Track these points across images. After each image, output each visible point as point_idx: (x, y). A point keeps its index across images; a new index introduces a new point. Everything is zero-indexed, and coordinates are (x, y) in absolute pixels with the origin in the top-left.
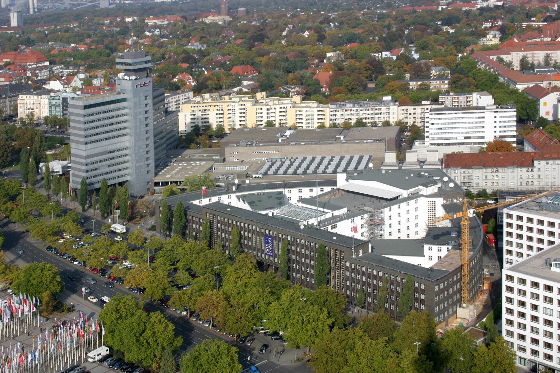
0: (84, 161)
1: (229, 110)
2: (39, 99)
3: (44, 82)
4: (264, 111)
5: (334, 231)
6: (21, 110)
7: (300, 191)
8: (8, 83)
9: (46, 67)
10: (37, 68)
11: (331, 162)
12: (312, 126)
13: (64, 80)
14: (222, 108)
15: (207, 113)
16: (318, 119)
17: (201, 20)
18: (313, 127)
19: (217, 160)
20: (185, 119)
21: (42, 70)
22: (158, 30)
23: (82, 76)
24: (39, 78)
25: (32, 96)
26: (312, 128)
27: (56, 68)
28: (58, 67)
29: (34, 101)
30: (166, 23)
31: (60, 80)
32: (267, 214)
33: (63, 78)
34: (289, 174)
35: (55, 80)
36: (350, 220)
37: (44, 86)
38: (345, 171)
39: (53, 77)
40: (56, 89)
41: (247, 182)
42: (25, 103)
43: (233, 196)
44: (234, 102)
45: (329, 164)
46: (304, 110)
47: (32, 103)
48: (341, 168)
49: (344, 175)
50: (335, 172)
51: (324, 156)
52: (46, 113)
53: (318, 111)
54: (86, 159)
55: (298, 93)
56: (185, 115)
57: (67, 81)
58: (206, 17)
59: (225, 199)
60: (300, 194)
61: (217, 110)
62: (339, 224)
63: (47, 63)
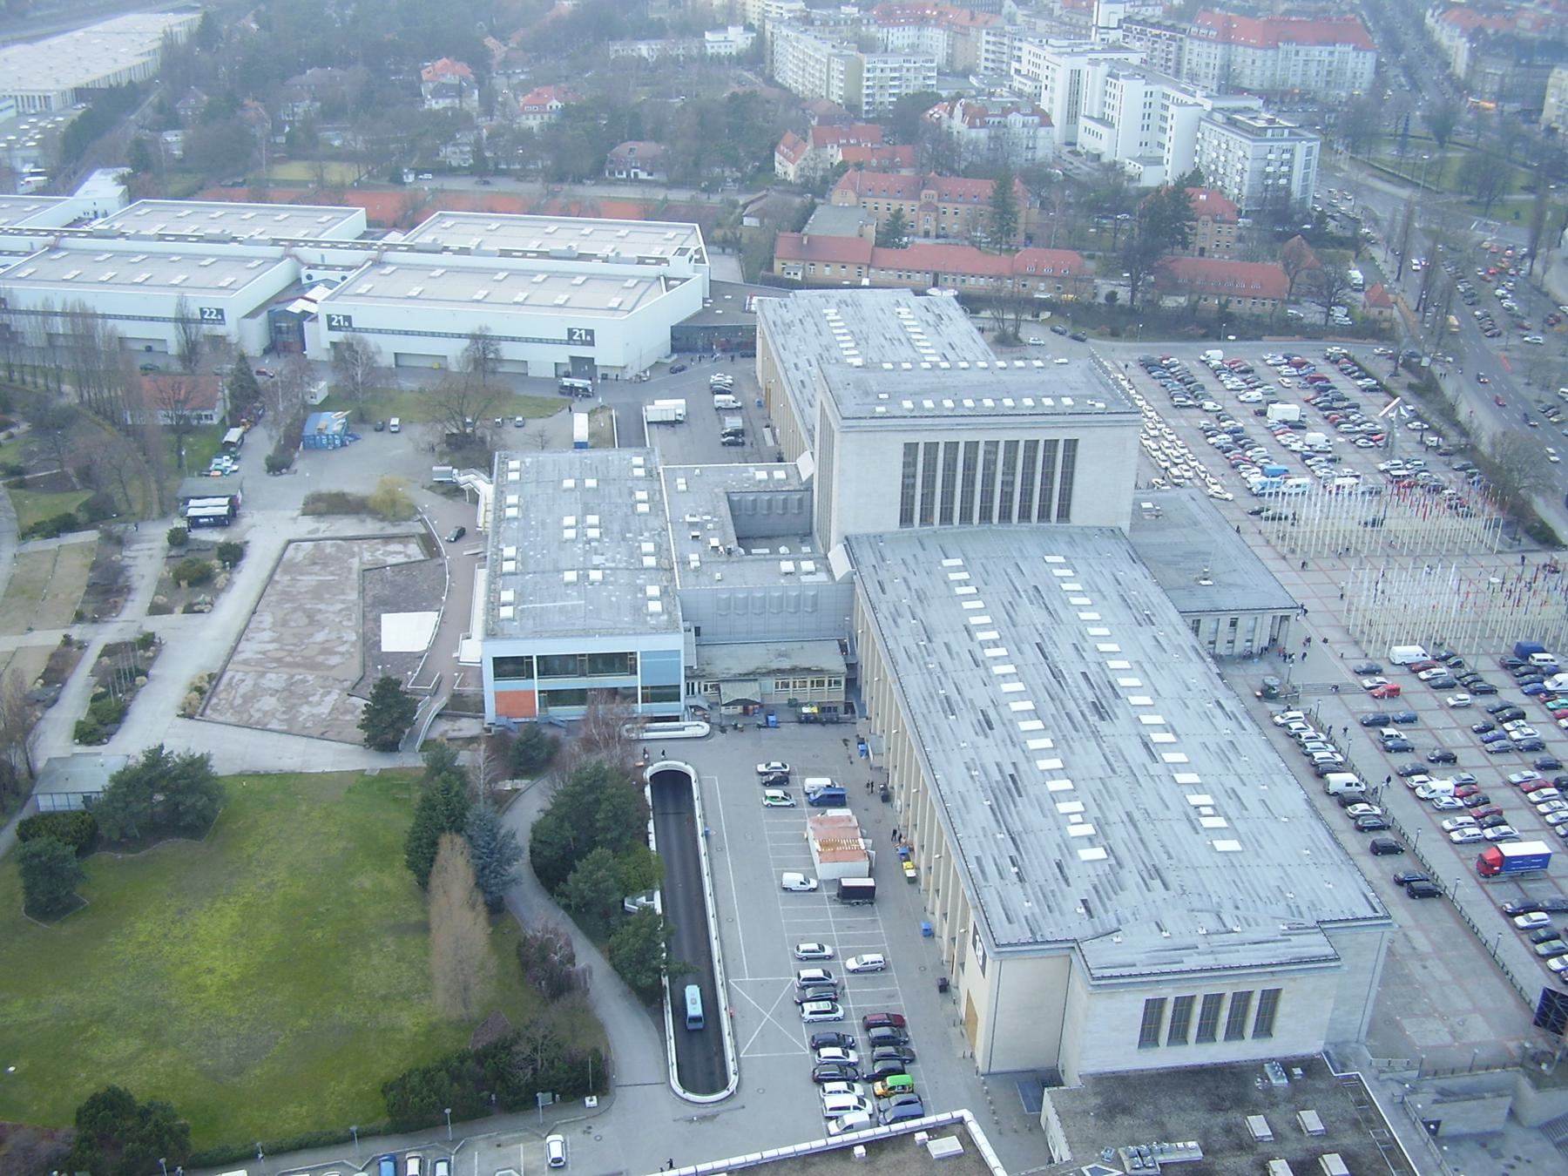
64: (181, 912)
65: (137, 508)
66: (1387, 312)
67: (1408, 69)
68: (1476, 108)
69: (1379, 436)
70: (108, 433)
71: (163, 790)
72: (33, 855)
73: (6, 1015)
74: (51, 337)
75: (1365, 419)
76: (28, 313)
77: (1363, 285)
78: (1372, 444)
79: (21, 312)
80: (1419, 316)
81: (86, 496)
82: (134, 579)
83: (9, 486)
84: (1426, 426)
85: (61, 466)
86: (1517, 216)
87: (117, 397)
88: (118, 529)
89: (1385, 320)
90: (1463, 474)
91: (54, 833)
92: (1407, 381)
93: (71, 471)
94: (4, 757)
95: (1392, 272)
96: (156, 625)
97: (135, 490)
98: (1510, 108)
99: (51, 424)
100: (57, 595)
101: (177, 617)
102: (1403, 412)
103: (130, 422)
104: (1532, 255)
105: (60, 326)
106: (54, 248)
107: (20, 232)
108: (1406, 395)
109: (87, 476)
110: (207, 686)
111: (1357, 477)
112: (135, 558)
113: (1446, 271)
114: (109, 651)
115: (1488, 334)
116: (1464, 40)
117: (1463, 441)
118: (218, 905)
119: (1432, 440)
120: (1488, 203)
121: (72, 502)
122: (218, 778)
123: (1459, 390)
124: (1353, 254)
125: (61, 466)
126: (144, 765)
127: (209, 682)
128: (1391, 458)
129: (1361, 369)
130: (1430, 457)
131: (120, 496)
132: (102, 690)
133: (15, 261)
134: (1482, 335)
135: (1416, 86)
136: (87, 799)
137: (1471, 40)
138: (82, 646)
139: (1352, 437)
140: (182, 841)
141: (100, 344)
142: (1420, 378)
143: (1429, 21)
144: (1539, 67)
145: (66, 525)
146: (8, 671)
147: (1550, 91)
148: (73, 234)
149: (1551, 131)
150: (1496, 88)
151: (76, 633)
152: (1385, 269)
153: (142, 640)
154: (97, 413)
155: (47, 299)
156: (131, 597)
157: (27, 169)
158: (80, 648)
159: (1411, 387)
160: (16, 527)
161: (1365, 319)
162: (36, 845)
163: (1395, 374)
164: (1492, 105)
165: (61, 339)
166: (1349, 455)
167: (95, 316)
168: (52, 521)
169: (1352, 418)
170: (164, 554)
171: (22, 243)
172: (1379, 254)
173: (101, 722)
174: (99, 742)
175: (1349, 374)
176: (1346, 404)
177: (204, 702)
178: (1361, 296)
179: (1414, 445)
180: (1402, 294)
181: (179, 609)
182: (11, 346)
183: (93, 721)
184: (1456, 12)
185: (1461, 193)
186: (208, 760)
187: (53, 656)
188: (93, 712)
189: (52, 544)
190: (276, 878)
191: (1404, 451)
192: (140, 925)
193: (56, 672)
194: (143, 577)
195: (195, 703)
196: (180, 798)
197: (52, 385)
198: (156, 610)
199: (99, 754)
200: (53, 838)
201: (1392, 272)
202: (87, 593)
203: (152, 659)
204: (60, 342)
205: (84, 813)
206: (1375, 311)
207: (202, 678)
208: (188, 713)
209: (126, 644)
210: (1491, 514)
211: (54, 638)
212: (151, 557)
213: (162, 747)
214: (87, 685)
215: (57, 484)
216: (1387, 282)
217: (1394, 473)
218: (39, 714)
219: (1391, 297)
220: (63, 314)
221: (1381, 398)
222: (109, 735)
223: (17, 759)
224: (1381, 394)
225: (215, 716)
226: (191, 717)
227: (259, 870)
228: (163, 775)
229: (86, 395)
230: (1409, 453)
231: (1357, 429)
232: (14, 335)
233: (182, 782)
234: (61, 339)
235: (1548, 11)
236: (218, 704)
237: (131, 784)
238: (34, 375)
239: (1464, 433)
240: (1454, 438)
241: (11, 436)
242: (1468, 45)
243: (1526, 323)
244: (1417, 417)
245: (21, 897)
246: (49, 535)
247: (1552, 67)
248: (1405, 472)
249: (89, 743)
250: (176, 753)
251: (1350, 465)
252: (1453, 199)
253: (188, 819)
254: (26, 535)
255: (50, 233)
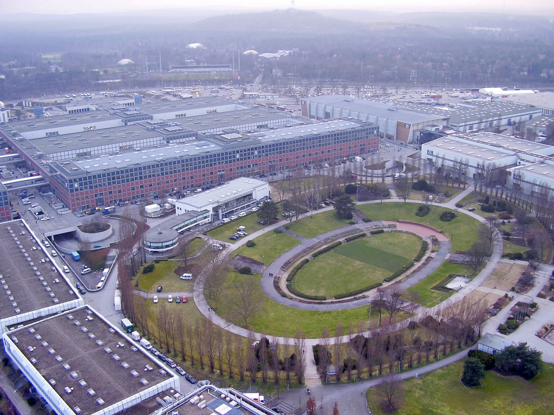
64: (512, 402)
65: (545, 259)
70: (542, 230)
71: (521, 358)
72: (470, 362)
73: (443, 410)
74: (533, 192)
76: (527, 182)
79: (525, 181)
81: (528, 249)
82: (536, 282)
83: (503, 238)
85: (523, 237)
87: (549, 218)
88: (536, 264)
91: (480, 358)
93: (526, 239)
94: (472, 327)
96: (538, 301)
97: (545, 253)
99: (524, 221)
100: (508, 280)
101: (547, 301)
103: (551, 228)
105: (537, 189)
106: (542, 163)
107: (532, 155)
109: (531, 243)
110: (549, 328)
112: (539, 275)
114: (519, 304)
118: (526, 406)
121: (522, 250)
122: (542, 362)
125: (523, 237)
126: (518, 347)
127: (550, 327)
131: (540, 253)
132: (512, 316)
133: (528, 164)
136: (494, 351)
138: (511, 299)
140: (522, 378)
141: (549, 199)
145: (518, 257)
146: (484, 299)
148: (550, 159)
151: (510, 294)
153: (532, 304)
154: (541, 222)
155: (535, 179)
156: (533, 289)
157: (540, 134)
158: (510, 300)
160: (502, 252)
162: (473, 359)
165: (536, 194)
167: (550, 189)
168: (514, 254)
170: (549, 277)
171: (531, 158)
173: (508, 327)
174: (505, 334)
177: (546, 334)
181: (548, 298)
182: (518, 192)
183: (506, 326)
186: (541, 354)
187: (500, 299)
188: (507, 323)
189: (512, 262)
190: (550, 405)
192: (497, 401)
193: (499, 305)
194: (539, 283)
195: (543, 333)
196: (526, 363)
197: (528, 209)
198: (540, 296)
199: (504, 338)
200: (479, 359)
202: (518, 282)
203: (533, 312)
204: (535, 195)
205: (492, 355)
207: (548, 325)
208: (539, 335)
209: (526, 304)
211: (501, 293)
212: (544, 277)
213: (526, 343)
214: (508, 313)
215: (520, 242)
218: (489, 317)
220: (539, 186)
222: (510, 333)
223: (476, 329)
225: (548, 340)
226: (540, 337)
227: (545, 400)
228: (523, 353)
229: (539, 215)
232: (520, 189)
233: (529, 358)
234: (536, 194)
236: (551, 336)
237: (511, 352)
238: (523, 204)
241: (509, 222)
245: (461, 375)
246: (511, 259)
249: (502, 333)
250: (530, 347)
253: (527, 372)
254: (504, 256)
255: (542, 157)
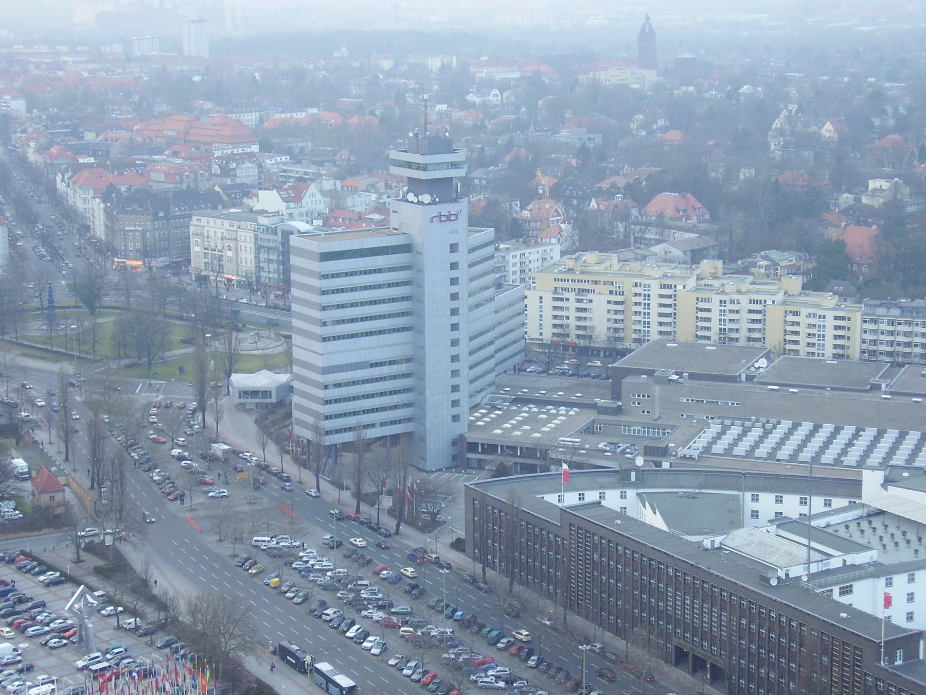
0: (320, 378)
1: (636, 295)
2: (234, 228)
3: (246, 191)
4: (715, 305)
5: (845, 600)
6: (197, 249)
7: (779, 500)
8: (172, 186)
9: (251, 155)
10: (231, 157)
11: (855, 442)
12: (821, 352)
13: (286, 190)
14: (621, 290)
15: (590, 296)
16: (836, 337)
17: (591, 75)
18: (823, 355)
19: (603, 407)
20: (541, 307)
21: (243, 163)
22: (497, 92)
23: (328, 184)
24: (238, 181)
25: (219, 221)
26: (821, 358)
27: (273, 161)
28: (278, 159)
29: (223, 231)
30: (517, 75)
31: (279, 189)
32: (699, 544)
33: (286, 186)
34: (757, 458)
35: (269, 189)
36: (882, 581)
37: (245, 200)
38: (884, 464)
39: (268, 182)
40: (271, 209)
41: (666, 465)
42: (206, 234)
43: (631, 493)
44: (649, 277)
45: (850, 444)
46: (804, 311)
47: (219, 235)
48: (876, 457)
49: (880, 476)
50: (861, 463)
51: (842, 425)
52: (249, 261)
53: (836, 318)
54: (323, 374)
55: (794, 271)
56: (541, 298)
57: (295, 196)
58: (605, 69)
59: (613, 499)
60: (779, 508)
61: (611, 293)
62: (858, 586)
63: (255, 148)
66: (58, 497)
67: (45, 239)
68: (123, 269)
69: (72, 631)
75: (53, 616)
77: (29, 473)
78: (65, 641)
80: (94, 494)
84: (120, 609)
86: (182, 370)
89: (59, 505)
90: (167, 650)
92: (92, 566)
95: (59, 452)
98: (158, 262)
102: (90, 600)
104: (202, 408)
108: (93, 580)
111: (52, 682)
113: (113, 443)
115: (171, 497)
116: (98, 200)
117: (162, 615)
119: (130, 621)
120: (150, 364)
123: (147, 564)
124: (14, 441)
128: (89, 651)
129: (41, 563)
130: (129, 641)
134: (165, 500)
135: (56, 255)
137: (104, 201)
139: (42, 640)
142: (105, 558)
143: (61, 186)
144: (179, 217)
147: (193, 240)
149: (202, 280)
150: (139, 245)
152: (51, 451)
159: (98, 571)
161: (37, 509)
163: (78, 561)
164: (139, 263)
166: (42, 660)
169: (39, 618)
172: (41, 435)
175: (29, 571)
176: (30, 604)
178: (28, 485)
179: (110, 632)
180: (73, 474)
184: (86, 173)
185: (120, 357)
191: (104, 641)
201: (59, 452)
206: (45, 498)
210: (203, 687)
216: (53, 463)
217: (94, 667)
219: (62, 480)
221: (67, 588)
224: (68, 585)
230: (107, 642)
231: (47, 629)
235: (179, 161)
239: (162, 606)
240: (152, 614)
242: (102, 205)
243: (208, 479)
244: (108, 600)
247: (190, 216)
248: (105, 664)
251: (44, 670)
252: (113, 365)
